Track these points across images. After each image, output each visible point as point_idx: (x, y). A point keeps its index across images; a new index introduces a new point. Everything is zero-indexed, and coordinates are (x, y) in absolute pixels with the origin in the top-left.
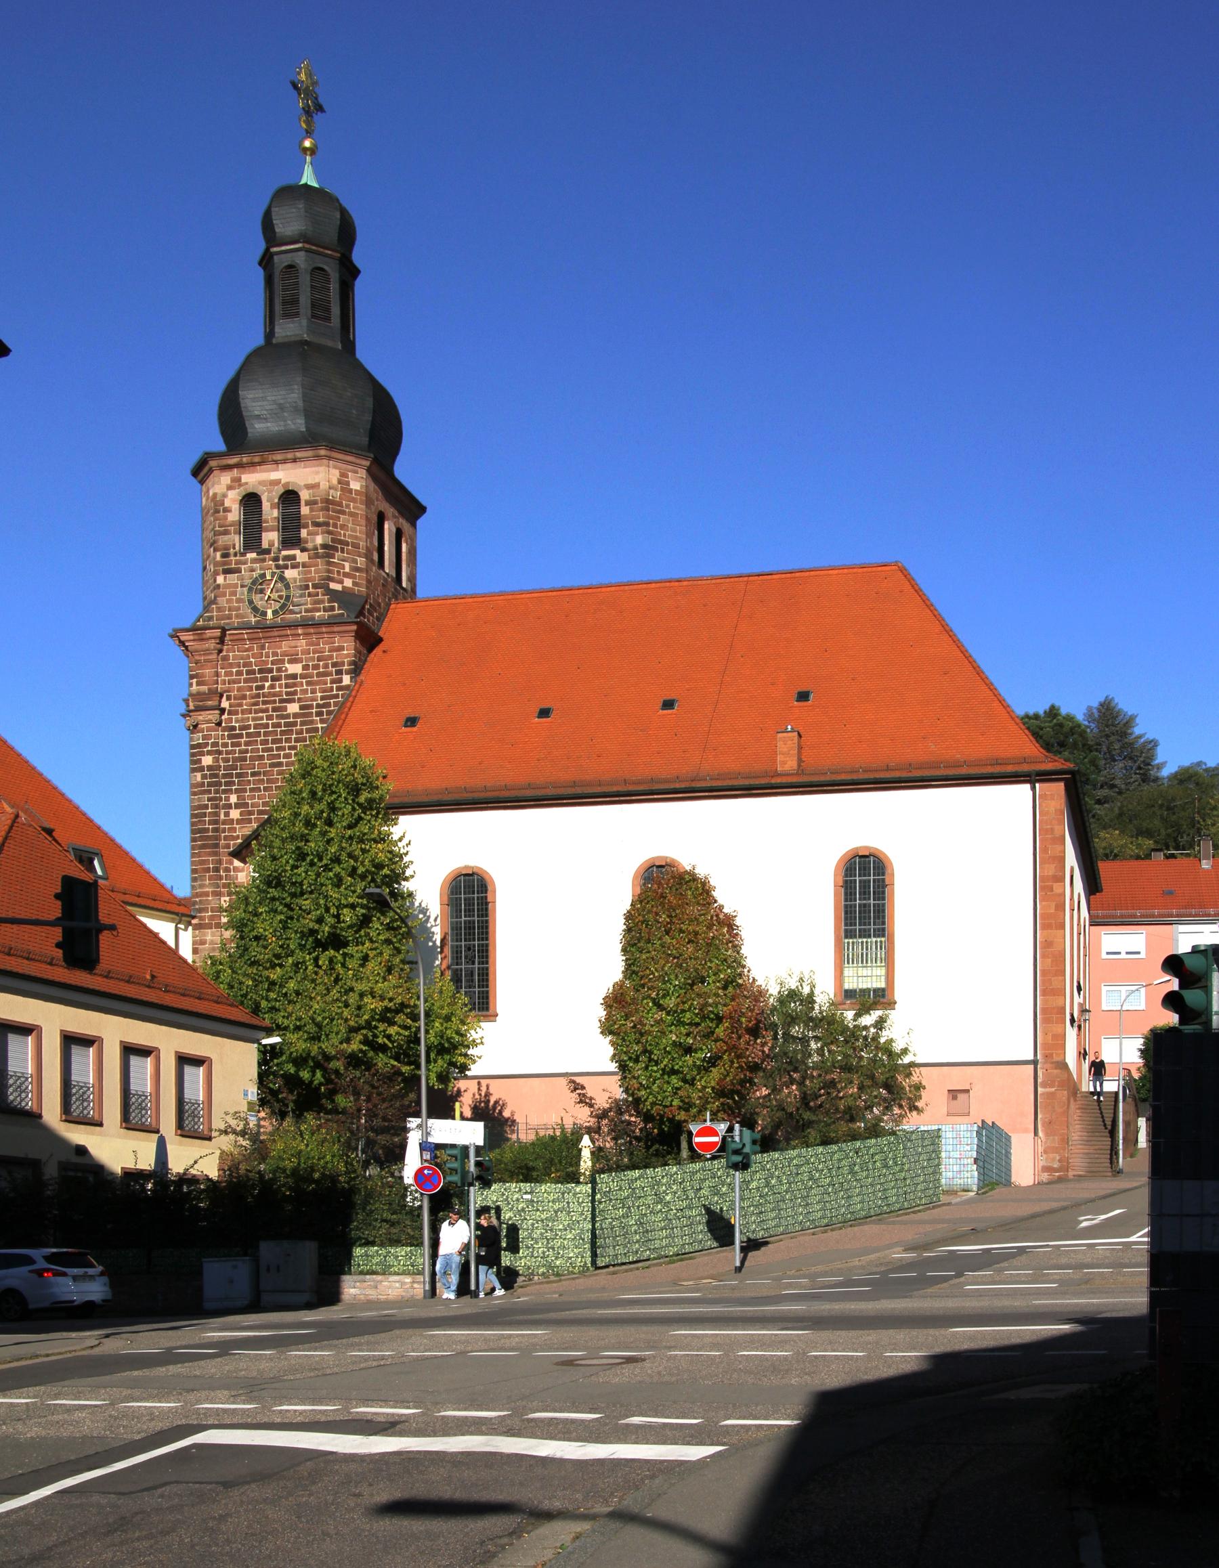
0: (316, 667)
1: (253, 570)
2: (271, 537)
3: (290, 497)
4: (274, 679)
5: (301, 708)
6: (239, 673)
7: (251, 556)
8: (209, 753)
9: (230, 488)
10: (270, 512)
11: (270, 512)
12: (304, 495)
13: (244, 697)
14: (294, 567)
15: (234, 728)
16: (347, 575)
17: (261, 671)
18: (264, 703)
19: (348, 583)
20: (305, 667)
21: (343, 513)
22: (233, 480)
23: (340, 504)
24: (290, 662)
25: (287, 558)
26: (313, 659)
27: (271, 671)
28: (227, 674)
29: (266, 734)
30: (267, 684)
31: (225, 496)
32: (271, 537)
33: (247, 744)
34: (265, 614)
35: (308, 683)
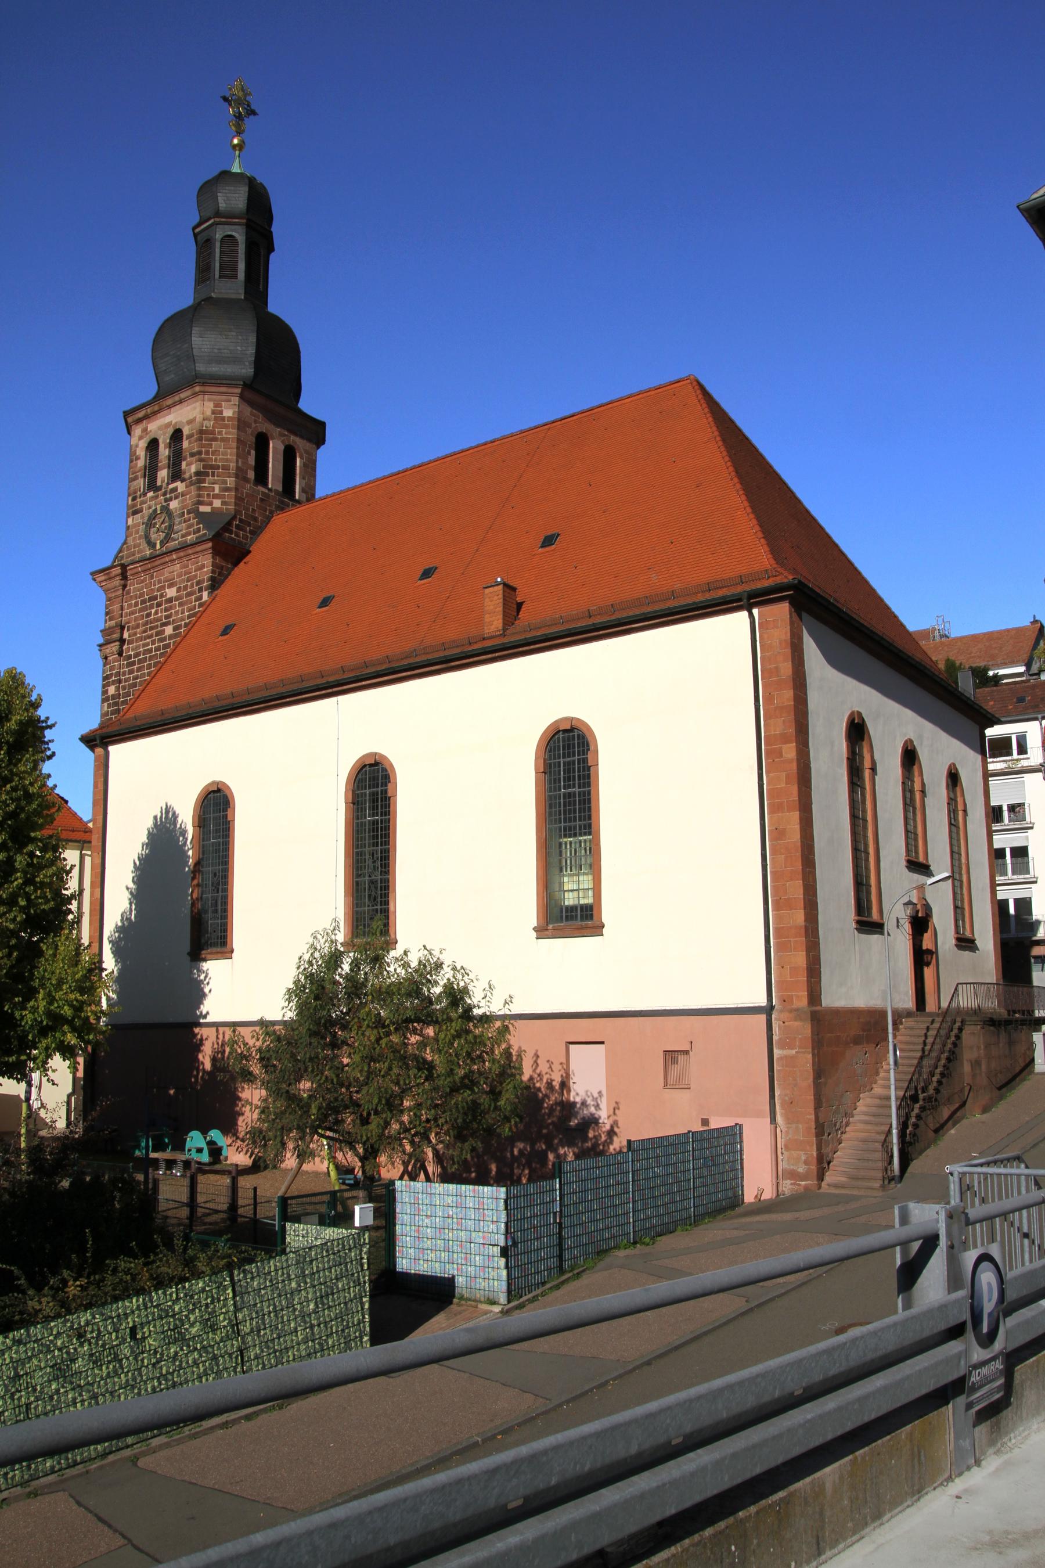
1: (150, 508)
2: (163, 474)
5: (175, 629)
6: (136, 604)
7: (151, 494)
8: (113, 683)
9: (141, 438)
10: (164, 452)
11: (164, 452)
12: (186, 431)
13: (138, 626)
14: (176, 497)
15: (129, 657)
16: (216, 497)
17: (150, 599)
18: (151, 628)
19: (217, 503)
21: (215, 439)
23: (213, 433)
24: (170, 587)
26: (183, 581)
27: (156, 598)
29: (151, 658)
30: (153, 611)
31: (137, 446)
32: (163, 474)
33: (138, 670)
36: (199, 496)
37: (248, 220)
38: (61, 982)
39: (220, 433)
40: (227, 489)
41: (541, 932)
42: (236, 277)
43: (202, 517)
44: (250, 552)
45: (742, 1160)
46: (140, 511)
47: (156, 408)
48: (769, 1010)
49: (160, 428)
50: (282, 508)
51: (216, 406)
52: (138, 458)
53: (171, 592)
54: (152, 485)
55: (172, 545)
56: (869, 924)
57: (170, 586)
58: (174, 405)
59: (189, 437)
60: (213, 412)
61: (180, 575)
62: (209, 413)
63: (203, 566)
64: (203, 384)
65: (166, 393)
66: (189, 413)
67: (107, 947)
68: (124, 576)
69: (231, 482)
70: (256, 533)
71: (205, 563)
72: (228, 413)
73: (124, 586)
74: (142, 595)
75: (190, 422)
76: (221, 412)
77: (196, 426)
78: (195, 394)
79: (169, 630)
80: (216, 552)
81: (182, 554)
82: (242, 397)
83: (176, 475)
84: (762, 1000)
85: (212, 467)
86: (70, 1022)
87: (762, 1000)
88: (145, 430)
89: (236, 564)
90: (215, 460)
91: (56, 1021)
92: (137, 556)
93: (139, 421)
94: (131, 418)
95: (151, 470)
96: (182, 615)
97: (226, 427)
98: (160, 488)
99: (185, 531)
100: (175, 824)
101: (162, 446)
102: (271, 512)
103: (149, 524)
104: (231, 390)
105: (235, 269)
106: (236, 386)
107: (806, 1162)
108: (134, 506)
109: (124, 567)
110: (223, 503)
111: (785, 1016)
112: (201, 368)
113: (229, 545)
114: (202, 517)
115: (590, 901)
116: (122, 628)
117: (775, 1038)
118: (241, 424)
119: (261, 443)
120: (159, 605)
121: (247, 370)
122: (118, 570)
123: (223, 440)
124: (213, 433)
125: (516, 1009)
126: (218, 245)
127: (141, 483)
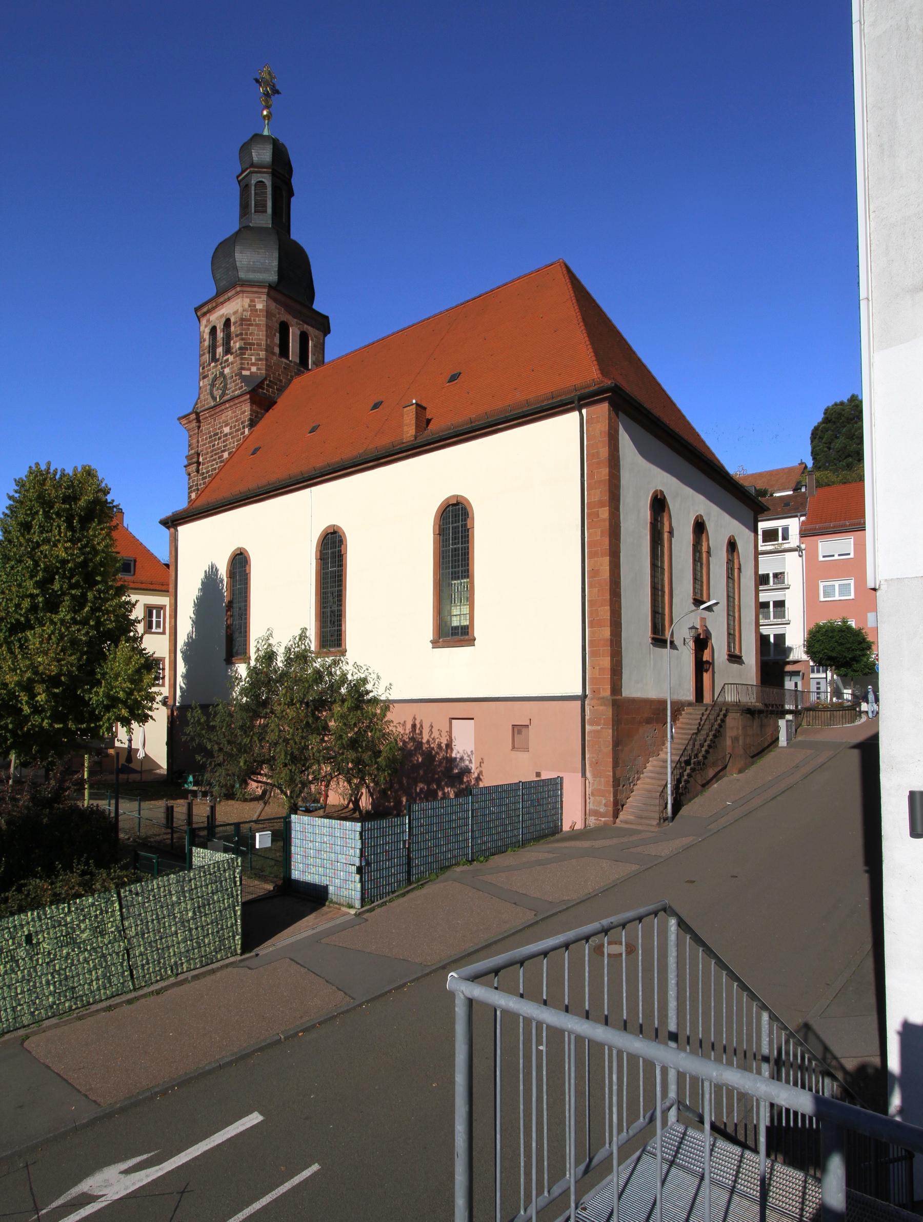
2: (220, 350)
7: (213, 364)
9: (206, 326)
10: (220, 335)
11: (220, 335)
12: (233, 320)
13: (207, 453)
15: (203, 474)
16: (253, 364)
18: (216, 454)
19: (254, 369)
21: (251, 325)
23: (250, 320)
27: (217, 434)
28: (202, 440)
32: (220, 350)
35: (232, 438)
36: (242, 364)
37: (273, 170)
38: (117, 675)
39: (255, 320)
40: (260, 360)
41: (435, 644)
42: (265, 211)
43: (244, 379)
44: (275, 403)
45: (562, 801)
47: (214, 305)
48: (584, 697)
49: (217, 319)
50: (299, 373)
51: (252, 301)
52: (205, 340)
53: (227, 430)
54: (214, 359)
55: (226, 398)
56: (659, 640)
57: (226, 426)
58: (225, 302)
59: (235, 323)
60: (250, 306)
61: (231, 418)
62: (246, 306)
63: (245, 412)
64: (242, 286)
65: (222, 293)
66: (234, 307)
67: (179, 656)
68: (199, 421)
69: (262, 354)
70: (281, 390)
71: (246, 409)
72: (260, 306)
73: (199, 427)
74: (209, 433)
75: (235, 313)
76: (255, 306)
77: (239, 315)
78: (237, 293)
79: (226, 455)
80: (253, 401)
81: (232, 404)
82: (268, 295)
83: (228, 351)
84: (578, 691)
85: (250, 344)
86: (124, 703)
87: (578, 691)
88: (208, 321)
89: (267, 410)
90: (253, 339)
91: (113, 702)
92: (206, 407)
93: (205, 314)
94: (201, 311)
95: (213, 348)
96: (233, 444)
97: (259, 316)
99: (235, 388)
100: (217, 575)
101: (218, 331)
102: (292, 377)
103: (213, 385)
104: (260, 290)
105: (265, 206)
106: (264, 287)
107: (605, 805)
108: (203, 373)
109: (197, 414)
110: (258, 369)
111: (594, 702)
112: (242, 275)
113: (262, 397)
114: (244, 379)
115: (466, 623)
116: (198, 455)
117: (587, 717)
118: (269, 314)
119: (284, 329)
120: (219, 439)
121: (273, 277)
122: (193, 416)
123: (257, 325)
124: (250, 320)
125: (394, 695)
126: (253, 188)
127: (207, 357)
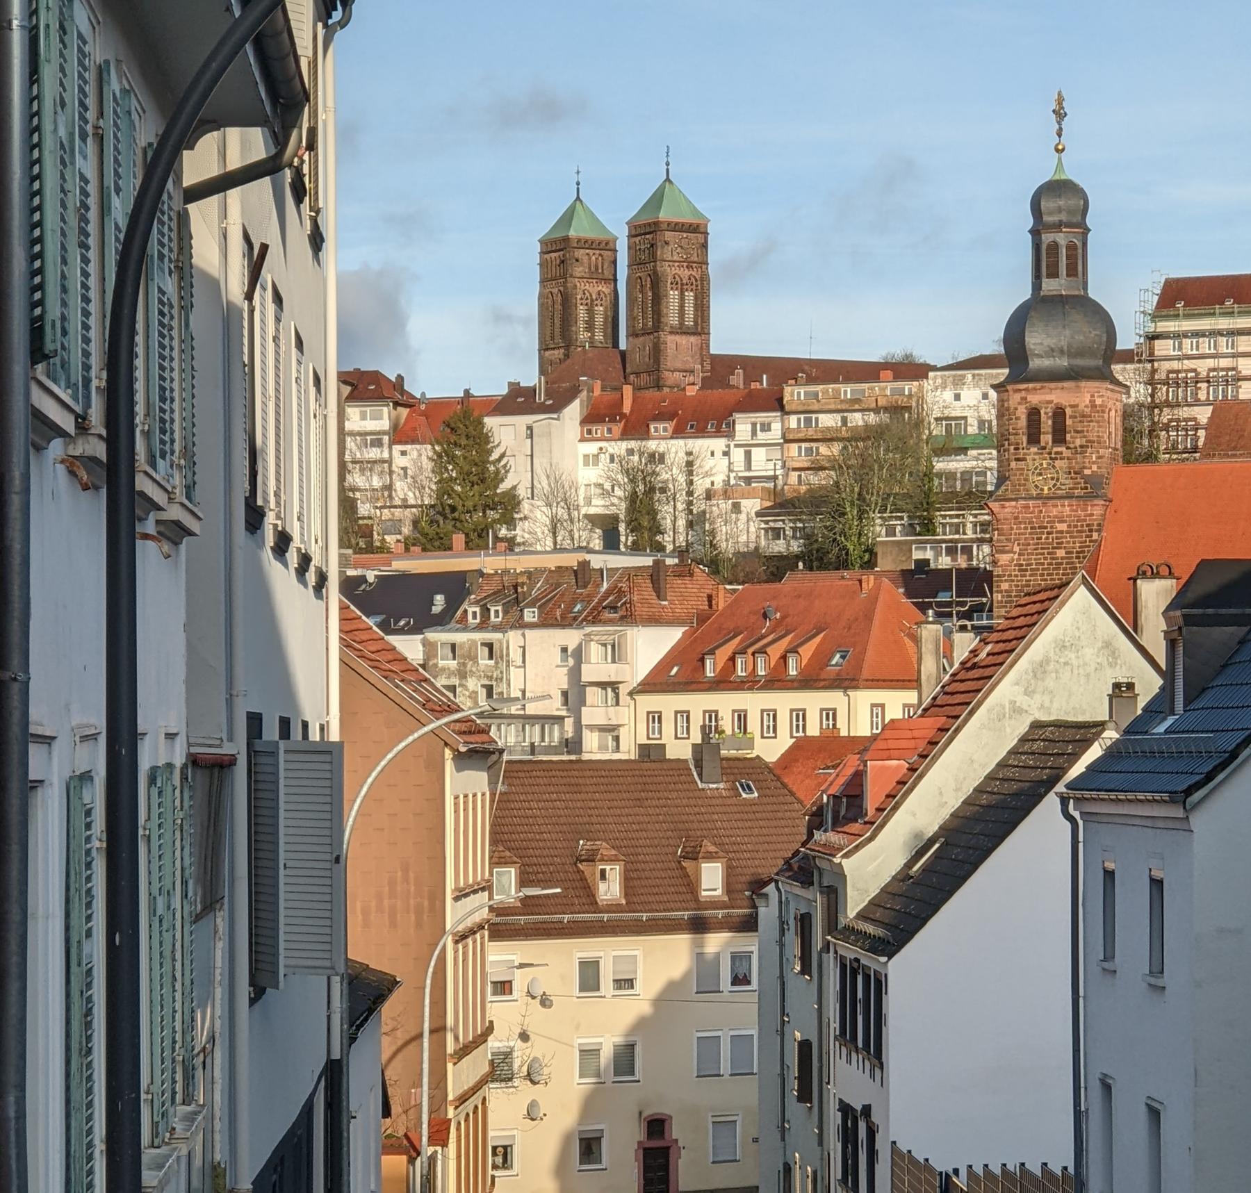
0: (1076, 526)
2: (1047, 438)
3: (1059, 414)
4: (1048, 533)
6: (1026, 528)
10: (1047, 423)
11: (1047, 423)
12: (1068, 411)
16: (1094, 463)
19: (1095, 468)
20: (1069, 526)
22: (1022, 398)
25: (1057, 453)
32: (1047, 438)
34: (1042, 490)
46: (1024, 459)
53: (1063, 527)
54: (1034, 439)
75: (1071, 406)
79: (1061, 553)
98: (1044, 448)
120: (1048, 533)
